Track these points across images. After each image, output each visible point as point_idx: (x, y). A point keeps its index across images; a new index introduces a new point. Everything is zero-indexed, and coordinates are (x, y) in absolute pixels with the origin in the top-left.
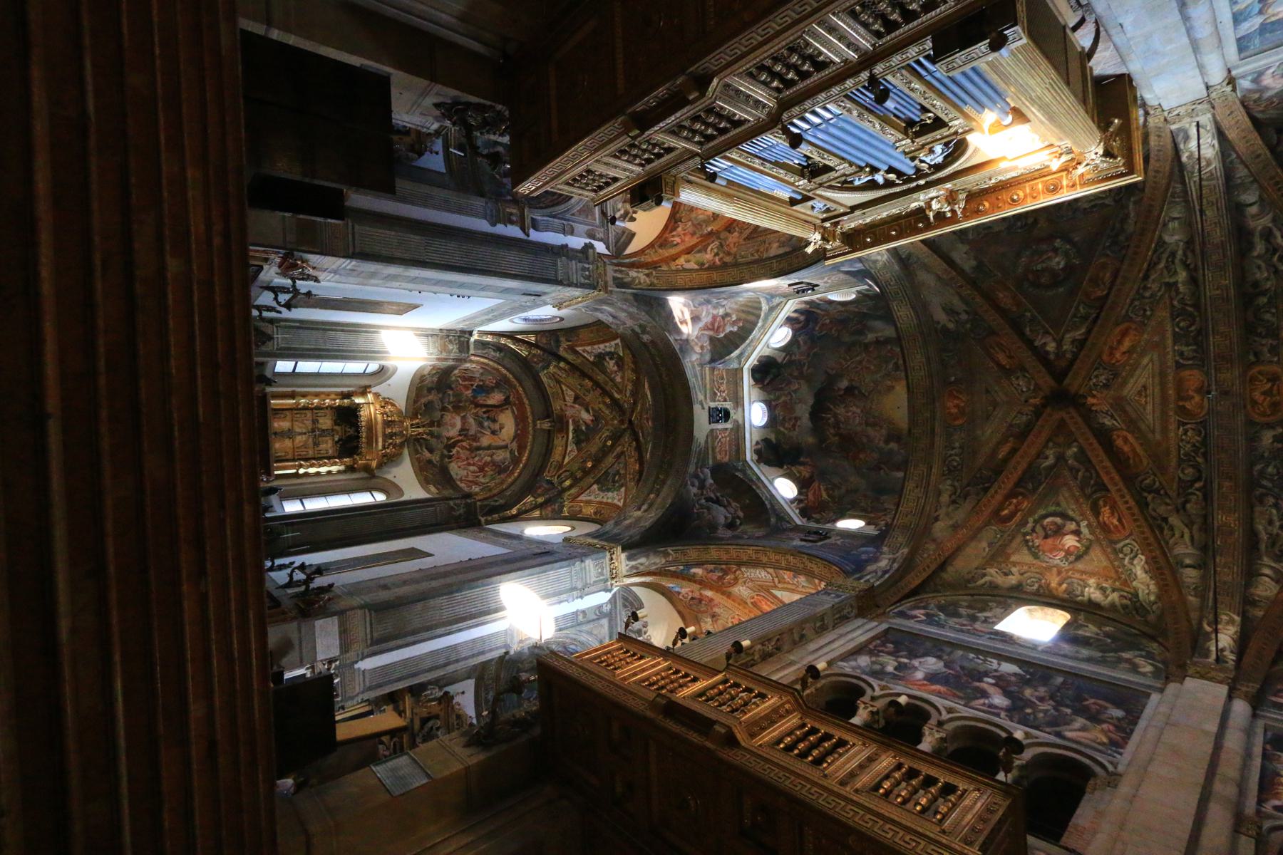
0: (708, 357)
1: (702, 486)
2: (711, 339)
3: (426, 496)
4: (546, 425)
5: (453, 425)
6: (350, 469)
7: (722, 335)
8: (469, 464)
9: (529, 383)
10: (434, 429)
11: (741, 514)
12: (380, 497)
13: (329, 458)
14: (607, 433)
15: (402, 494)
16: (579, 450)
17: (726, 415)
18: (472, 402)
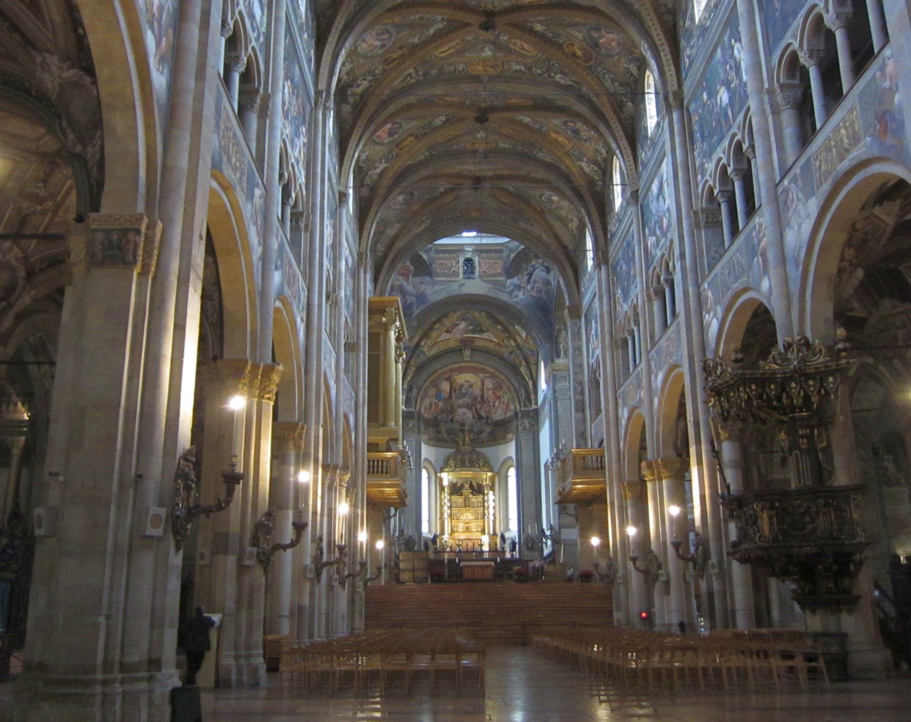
0: (427, 278)
1: (518, 287)
2: (416, 275)
3: (514, 442)
4: (467, 353)
5: (464, 414)
6: (492, 488)
7: (412, 268)
8: (494, 405)
9: (436, 365)
10: (466, 428)
11: (540, 261)
12: (512, 472)
13: (484, 501)
14: (476, 313)
15: (510, 458)
16: (487, 331)
17: (468, 261)
18: (448, 401)
